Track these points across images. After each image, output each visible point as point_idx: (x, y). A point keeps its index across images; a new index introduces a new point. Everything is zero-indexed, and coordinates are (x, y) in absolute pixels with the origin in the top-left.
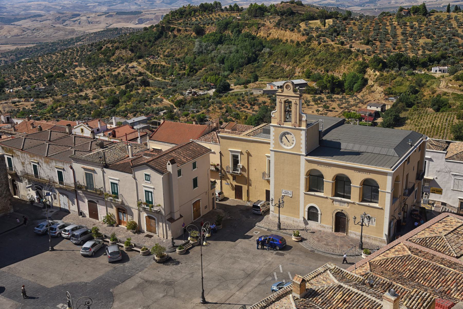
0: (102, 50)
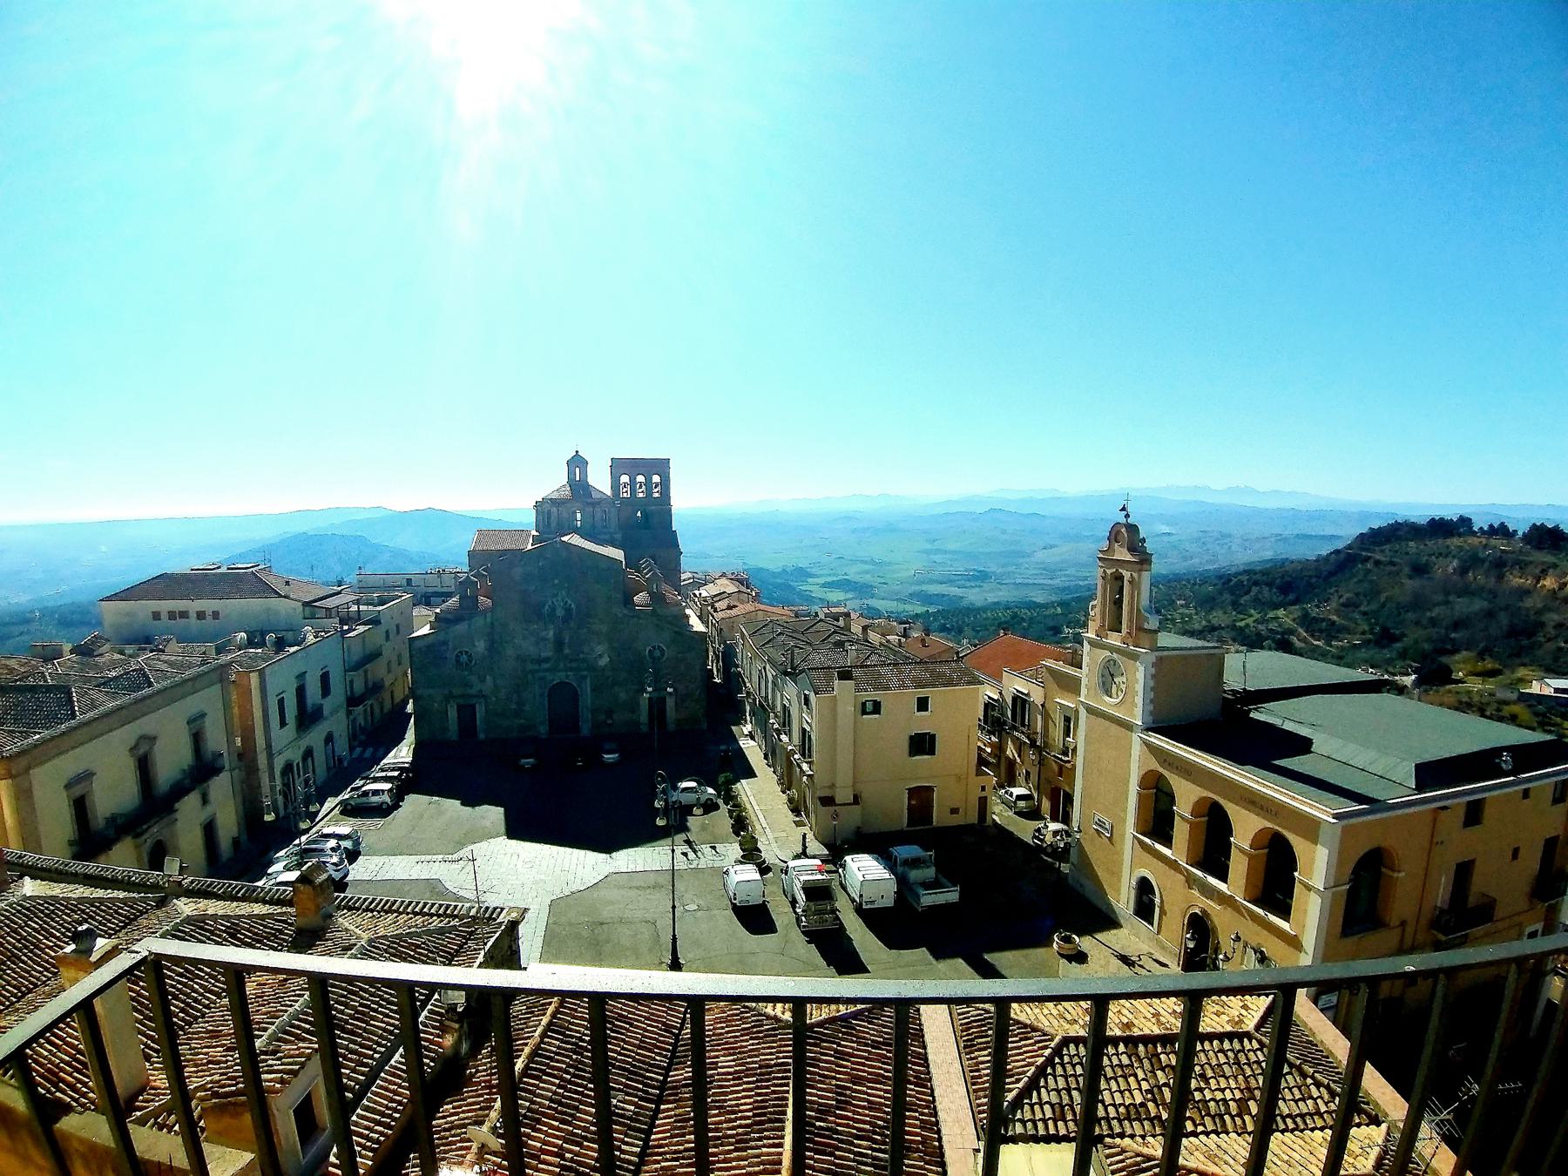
0: (1232, 583)
